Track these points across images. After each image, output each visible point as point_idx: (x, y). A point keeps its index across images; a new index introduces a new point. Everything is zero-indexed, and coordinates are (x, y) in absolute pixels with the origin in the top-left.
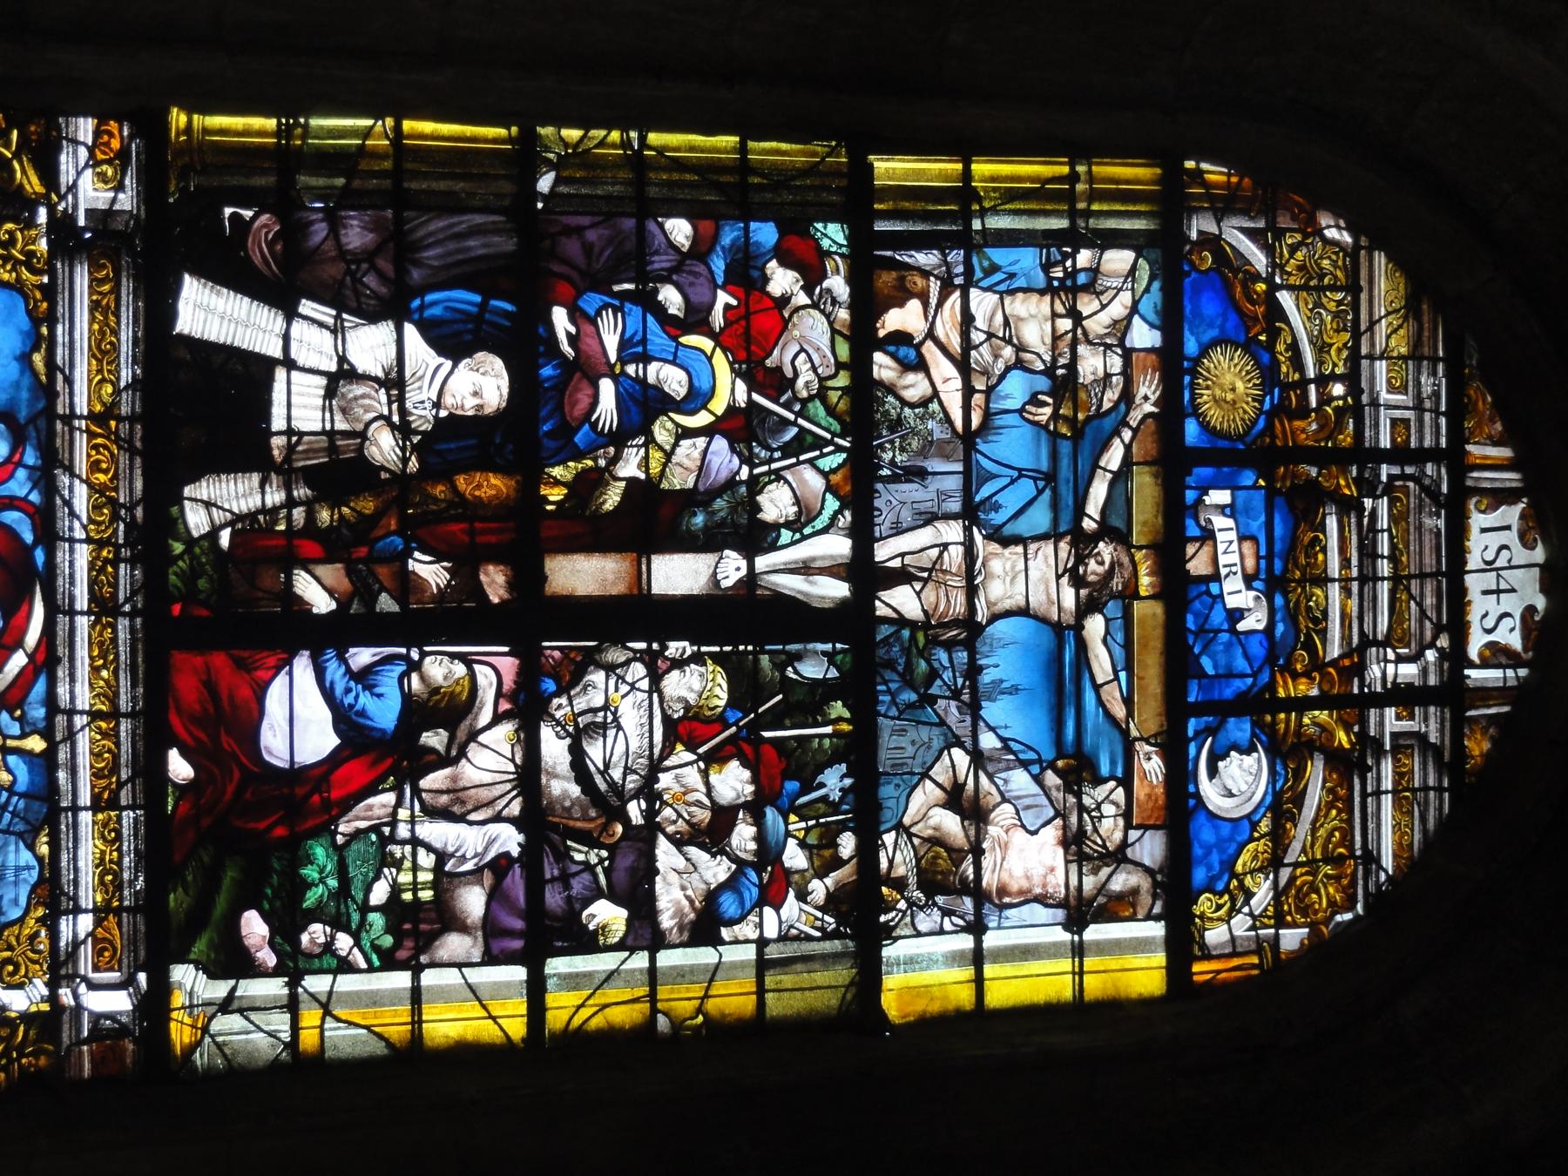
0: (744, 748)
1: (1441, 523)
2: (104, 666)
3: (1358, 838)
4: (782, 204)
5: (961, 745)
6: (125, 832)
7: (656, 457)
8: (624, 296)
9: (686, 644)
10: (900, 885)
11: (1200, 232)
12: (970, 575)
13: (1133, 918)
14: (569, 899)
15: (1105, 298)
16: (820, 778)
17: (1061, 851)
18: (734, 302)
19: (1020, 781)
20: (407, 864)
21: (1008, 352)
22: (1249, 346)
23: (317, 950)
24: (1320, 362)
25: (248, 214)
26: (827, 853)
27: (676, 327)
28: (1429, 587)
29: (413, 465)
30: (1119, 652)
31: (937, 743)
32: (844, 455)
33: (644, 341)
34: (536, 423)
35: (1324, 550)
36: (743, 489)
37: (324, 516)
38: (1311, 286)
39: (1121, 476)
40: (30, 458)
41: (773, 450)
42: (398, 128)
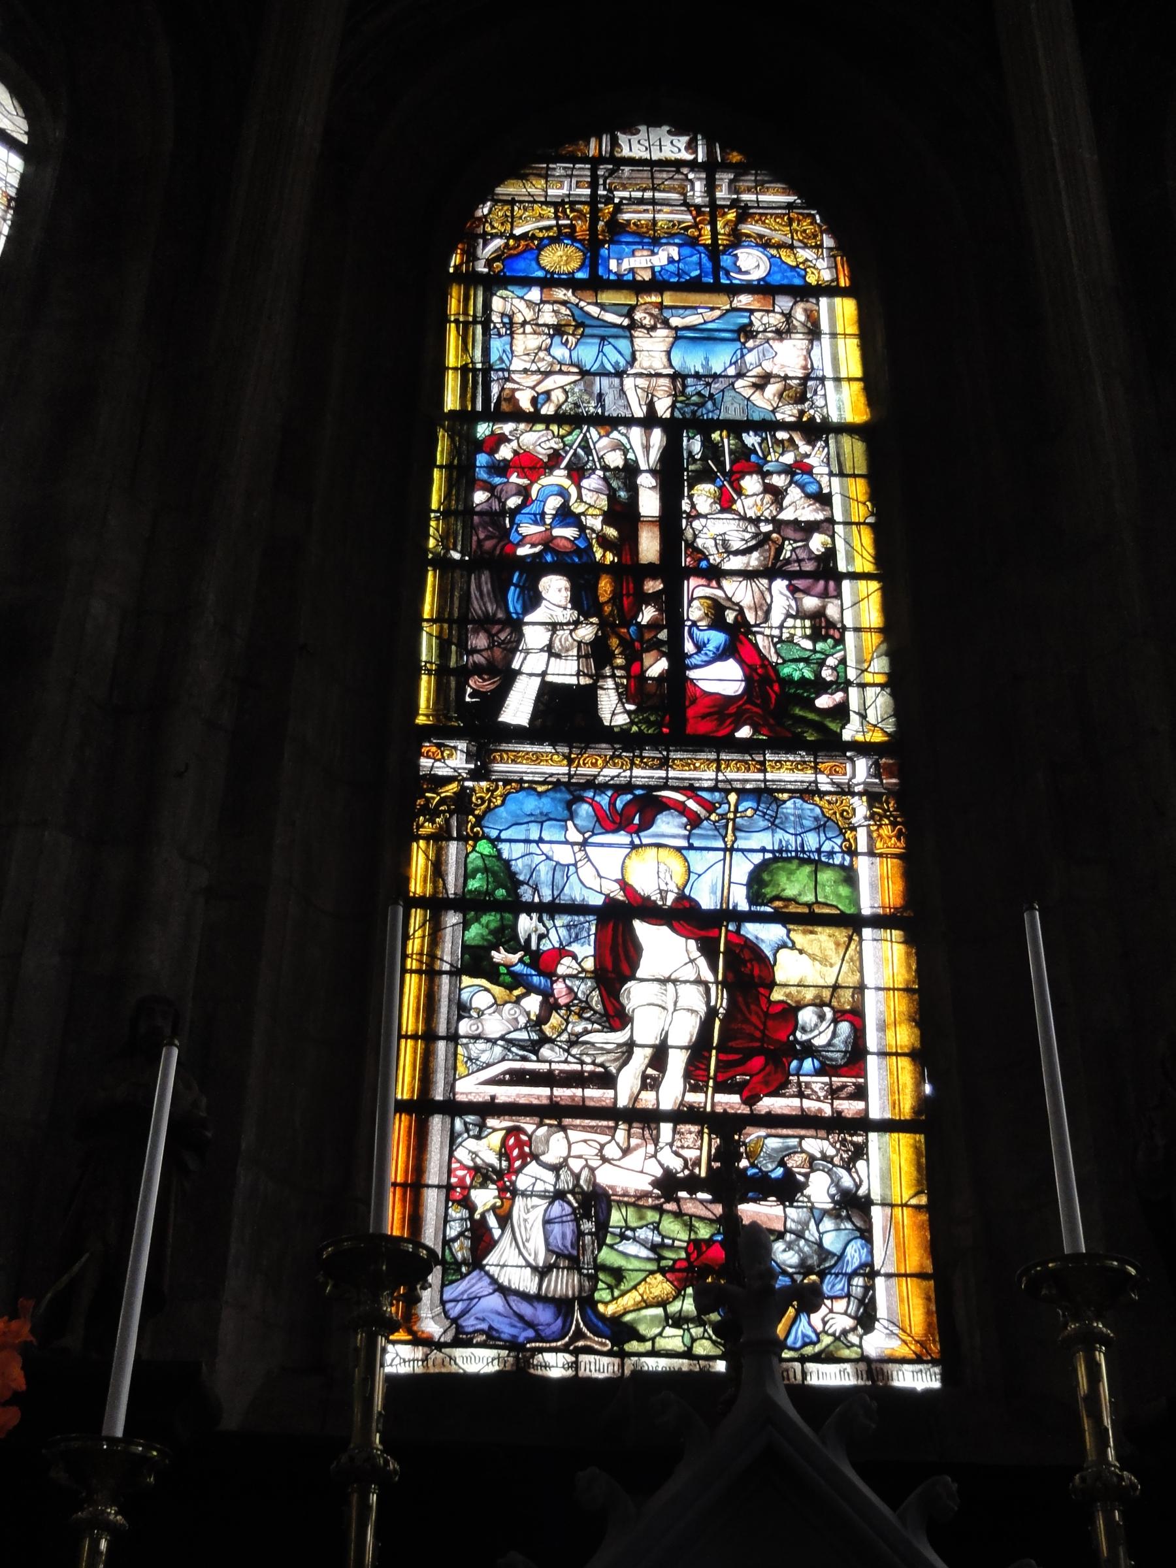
0: (734, 478)
1: (627, 169)
2: (694, 765)
3: (779, 211)
4: (468, 450)
5: (733, 384)
6: (776, 759)
7: (591, 511)
8: (512, 522)
9: (683, 502)
10: (802, 413)
11: (485, 267)
12: (650, 375)
13: (818, 312)
14: (809, 559)
15: (516, 311)
16: (750, 446)
17: (785, 341)
18: (516, 474)
19: (751, 358)
20: (792, 631)
21: (542, 354)
22: (540, 248)
23: (835, 673)
24: (548, 218)
25: (469, 690)
26: (786, 444)
27: (527, 500)
28: (657, 175)
29: (594, 620)
30: (688, 312)
31: (732, 393)
32: (592, 429)
33: (535, 515)
34: (574, 563)
35: (639, 220)
36: (608, 474)
37: (619, 661)
38: (512, 220)
39: (602, 307)
40: (590, 794)
41: (588, 460)
42: (427, 621)
